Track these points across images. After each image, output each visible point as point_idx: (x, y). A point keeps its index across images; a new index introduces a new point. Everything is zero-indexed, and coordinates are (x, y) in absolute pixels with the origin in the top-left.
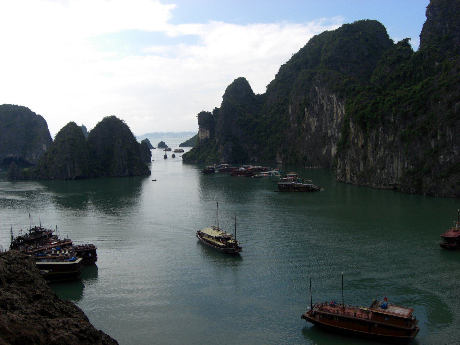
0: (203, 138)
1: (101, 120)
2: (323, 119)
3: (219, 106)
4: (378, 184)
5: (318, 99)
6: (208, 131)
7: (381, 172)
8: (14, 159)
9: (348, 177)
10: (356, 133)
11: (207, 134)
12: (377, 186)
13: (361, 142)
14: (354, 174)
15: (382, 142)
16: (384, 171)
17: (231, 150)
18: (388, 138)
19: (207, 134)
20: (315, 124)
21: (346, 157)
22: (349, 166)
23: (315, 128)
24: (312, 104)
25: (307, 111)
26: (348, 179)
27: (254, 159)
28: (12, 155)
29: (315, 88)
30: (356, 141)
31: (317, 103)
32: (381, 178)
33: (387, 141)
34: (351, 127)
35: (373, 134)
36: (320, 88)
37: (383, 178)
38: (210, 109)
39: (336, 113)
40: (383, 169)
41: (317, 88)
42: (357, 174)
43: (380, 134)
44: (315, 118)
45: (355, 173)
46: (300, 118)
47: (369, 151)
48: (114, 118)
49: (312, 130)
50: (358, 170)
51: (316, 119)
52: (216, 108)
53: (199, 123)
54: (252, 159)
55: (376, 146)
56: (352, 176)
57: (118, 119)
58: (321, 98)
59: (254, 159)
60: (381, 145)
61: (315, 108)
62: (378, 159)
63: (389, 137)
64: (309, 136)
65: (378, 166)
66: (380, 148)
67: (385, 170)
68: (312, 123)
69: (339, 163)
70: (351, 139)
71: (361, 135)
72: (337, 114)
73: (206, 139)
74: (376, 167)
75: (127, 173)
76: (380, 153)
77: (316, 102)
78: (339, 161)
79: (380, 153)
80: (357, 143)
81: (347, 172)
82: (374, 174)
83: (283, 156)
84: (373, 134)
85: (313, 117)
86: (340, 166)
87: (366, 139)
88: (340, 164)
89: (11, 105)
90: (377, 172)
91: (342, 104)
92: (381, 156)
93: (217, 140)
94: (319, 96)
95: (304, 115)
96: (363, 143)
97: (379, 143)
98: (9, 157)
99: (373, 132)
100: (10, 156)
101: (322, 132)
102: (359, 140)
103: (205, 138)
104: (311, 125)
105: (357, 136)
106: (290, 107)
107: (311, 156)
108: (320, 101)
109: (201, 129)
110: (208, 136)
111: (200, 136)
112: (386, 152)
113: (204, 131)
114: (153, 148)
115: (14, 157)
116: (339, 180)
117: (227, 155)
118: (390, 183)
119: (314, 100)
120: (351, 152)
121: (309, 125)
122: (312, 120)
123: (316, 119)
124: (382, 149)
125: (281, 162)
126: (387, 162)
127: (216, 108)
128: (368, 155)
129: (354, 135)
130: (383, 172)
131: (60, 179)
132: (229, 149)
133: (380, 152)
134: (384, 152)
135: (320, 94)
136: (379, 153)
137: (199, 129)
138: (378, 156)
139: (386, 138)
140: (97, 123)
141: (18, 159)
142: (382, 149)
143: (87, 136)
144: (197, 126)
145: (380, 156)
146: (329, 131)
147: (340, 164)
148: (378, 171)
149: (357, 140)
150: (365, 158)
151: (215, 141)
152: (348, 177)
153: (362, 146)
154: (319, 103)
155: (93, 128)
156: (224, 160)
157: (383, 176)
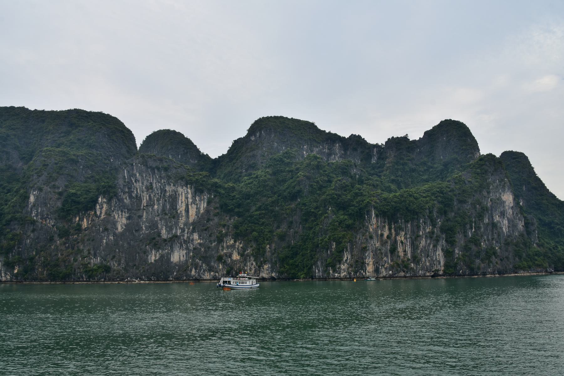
2: (142, 216)
23: (124, 227)
39: (185, 209)
41: (139, 175)
44: (124, 214)
49: (117, 229)
51: (127, 215)
68: (119, 220)
72: (187, 211)
85: (122, 211)
88: (347, 258)
91: (200, 200)
101: (141, 233)
104: (117, 222)
106: (33, 194)
146: (164, 231)
147: (347, 258)
154: (134, 195)
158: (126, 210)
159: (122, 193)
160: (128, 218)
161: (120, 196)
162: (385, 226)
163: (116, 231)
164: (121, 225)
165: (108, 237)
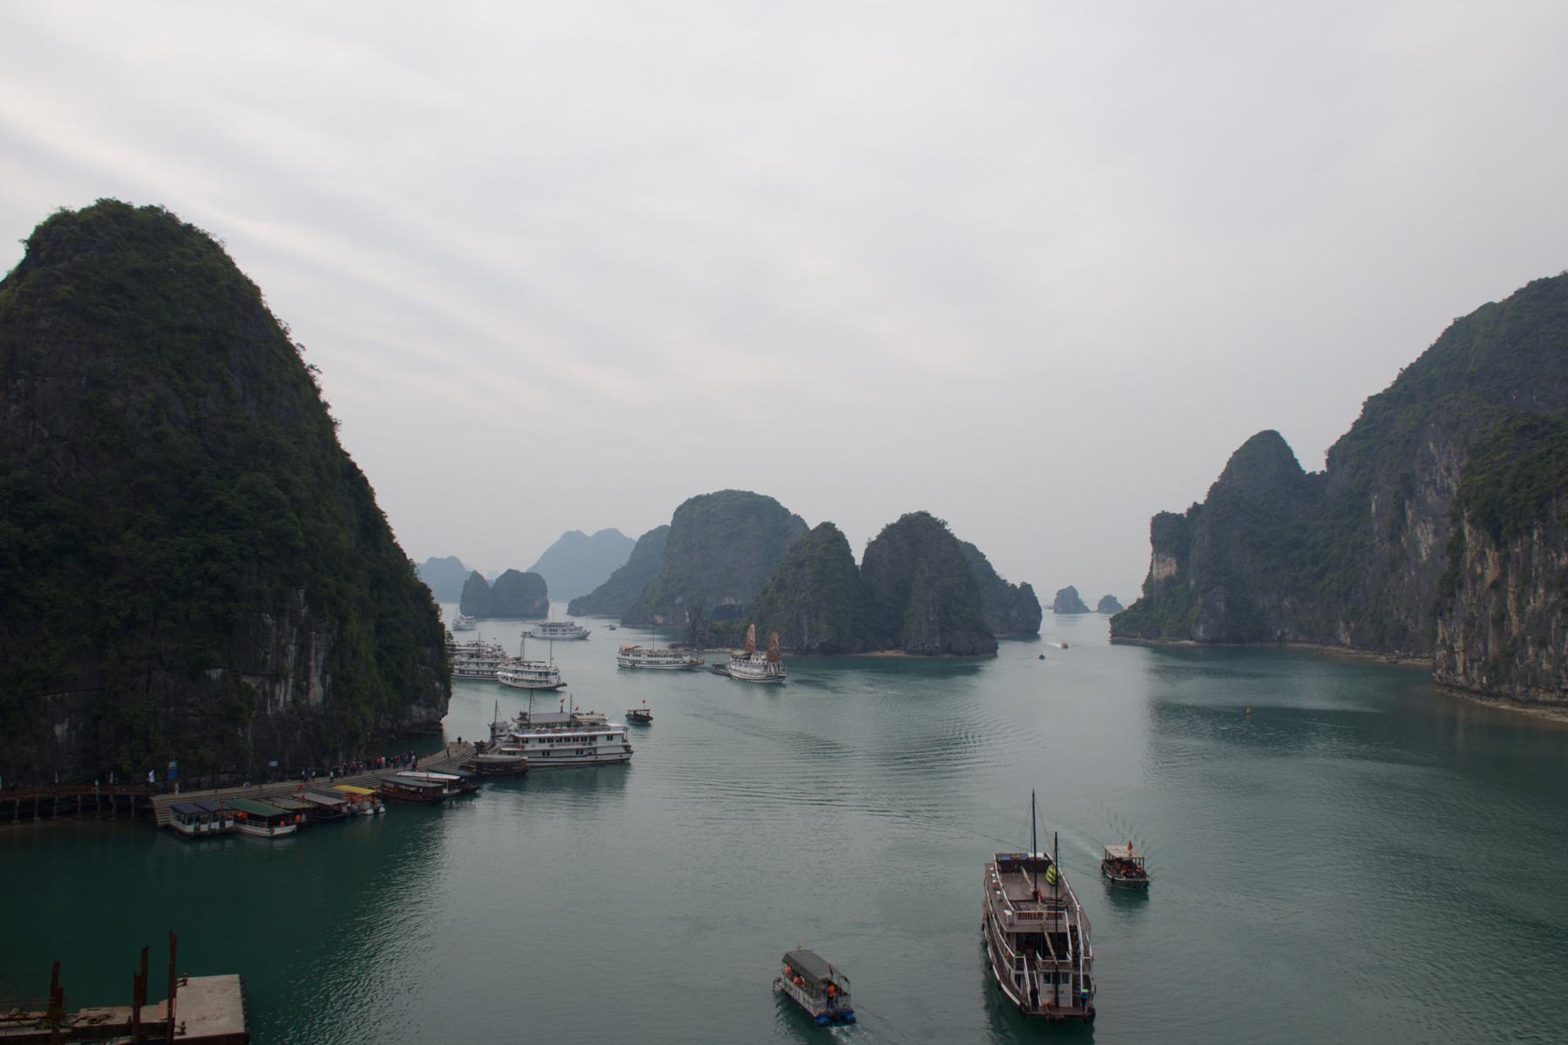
0: (1163, 575)
1: (895, 519)
3: (1201, 501)
4: (1529, 687)
5: (1436, 475)
6: (1173, 561)
7: (1537, 655)
8: (736, 610)
9: (1460, 669)
10: (1478, 548)
11: (1170, 568)
12: (1526, 692)
13: (1491, 575)
14: (1472, 661)
15: (1541, 569)
16: (1547, 650)
17: (1222, 607)
18: (1556, 560)
19: (1170, 568)
20: (1431, 541)
21: (1454, 613)
22: (1461, 638)
23: (1429, 552)
24: (1423, 490)
25: (1410, 507)
26: (1459, 675)
27: (1283, 634)
28: (733, 602)
29: (1428, 446)
30: (1479, 570)
31: (1435, 485)
32: (1539, 671)
33: (1556, 568)
34: (1466, 533)
35: (1517, 550)
36: (1441, 445)
37: (1542, 671)
38: (1180, 507)
40: (1542, 643)
42: (1480, 660)
43: (1536, 547)
44: (1428, 526)
45: (1476, 657)
46: (1397, 527)
47: (1511, 596)
48: (923, 516)
49: (1421, 556)
50: (1481, 650)
51: (1432, 527)
52: (1195, 503)
53: (1153, 541)
54: (1279, 633)
55: (1526, 582)
56: (1468, 665)
57: (933, 519)
58: (1442, 470)
59: (1283, 634)
60: (1536, 578)
61: (1429, 500)
62: (1529, 619)
63: (1559, 556)
64: (1413, 573)
65: (1529, 638)
66: (1536, 588)
67: (1550, 647)
68: (1422, 539)
69: (1440, 631)
70: (1468, 566)
71: (1491, 555)
73: (1169, 581)
74: (1524, 640)
75: (937, 644)
76: (1534, 602)
77: (1434, 482)
78: (1440, 626)
79: (1534, 604)
80: (1482, 576)
81: (1457, 656)
82: (1517, 659)
83: (1352, 625)
84: (1517, 550)
85: (1424, 521)
86: (1443, 640)
87: (1504, 562)
88: (1443, 634)
89: (740, 492)
90: (1527, 653)
92: (1538, 610)
93: (1192, 583)
94: (1438, 465)
95: (1404, 514)
96: (1497, 575)
97: (1534, 573)
98: (726, 605)
99: (1519, 543)
100: (727, 602)
102: (1486, 568)
103: (1166, 577)
104: (1419, 542)
105: (1481, 557)
107: (1416, 625)
108: (1442, 480)
109: (1157, 559)
110: (1173, 572)
111: (1154, 573)
112: (1551, 599)
113: (1164, 561)
114: (1086, 610)
115: (734, 606)
116: (1440, 677)
117: (1212, 621)
118: (1563, 687)
119: (1428, 478)
120: (1465, 598)
121: (1414, 544)
122: (1423, 530)
123: (1430, 527)
124: (1541, 591)
125: (1348, 641)
126: (1554, 625)
127: (1195, 503)
128: (1509, 608)
129: (1475, 552)
130: (1543, 652)
131: (785, 648)
132: (1218, 604)
133: (1534, 598)
134: (1546, 597)
135: (1440, 460)
136: (1532, 600)
137: (1152, 555)
138: (1529, 608)
139: (1553, 559)
140: (884, 526)
141: (743, 609)
142: (1541, 591)
143: (858, 556)
144: (1149, 548)
145: (1534, 608)
147: (1443, 634)
148: (1531, 651)
149: (1483, 568)
150: (1501, 618)
151: (1188, 585)
152: (1460, 669)
153: (1495, 585)
154: (1438, 486)
155: (874, 539)
156: (1204, 632)
157: (1544, 665)
158: (1430, 518)
159: (1423, 486)
160: (1436, 533)
161: (1420, 492)
162: (1484, 553)
163: (1420, 561)
164: (1426, 548)
165: (1410, 573)
